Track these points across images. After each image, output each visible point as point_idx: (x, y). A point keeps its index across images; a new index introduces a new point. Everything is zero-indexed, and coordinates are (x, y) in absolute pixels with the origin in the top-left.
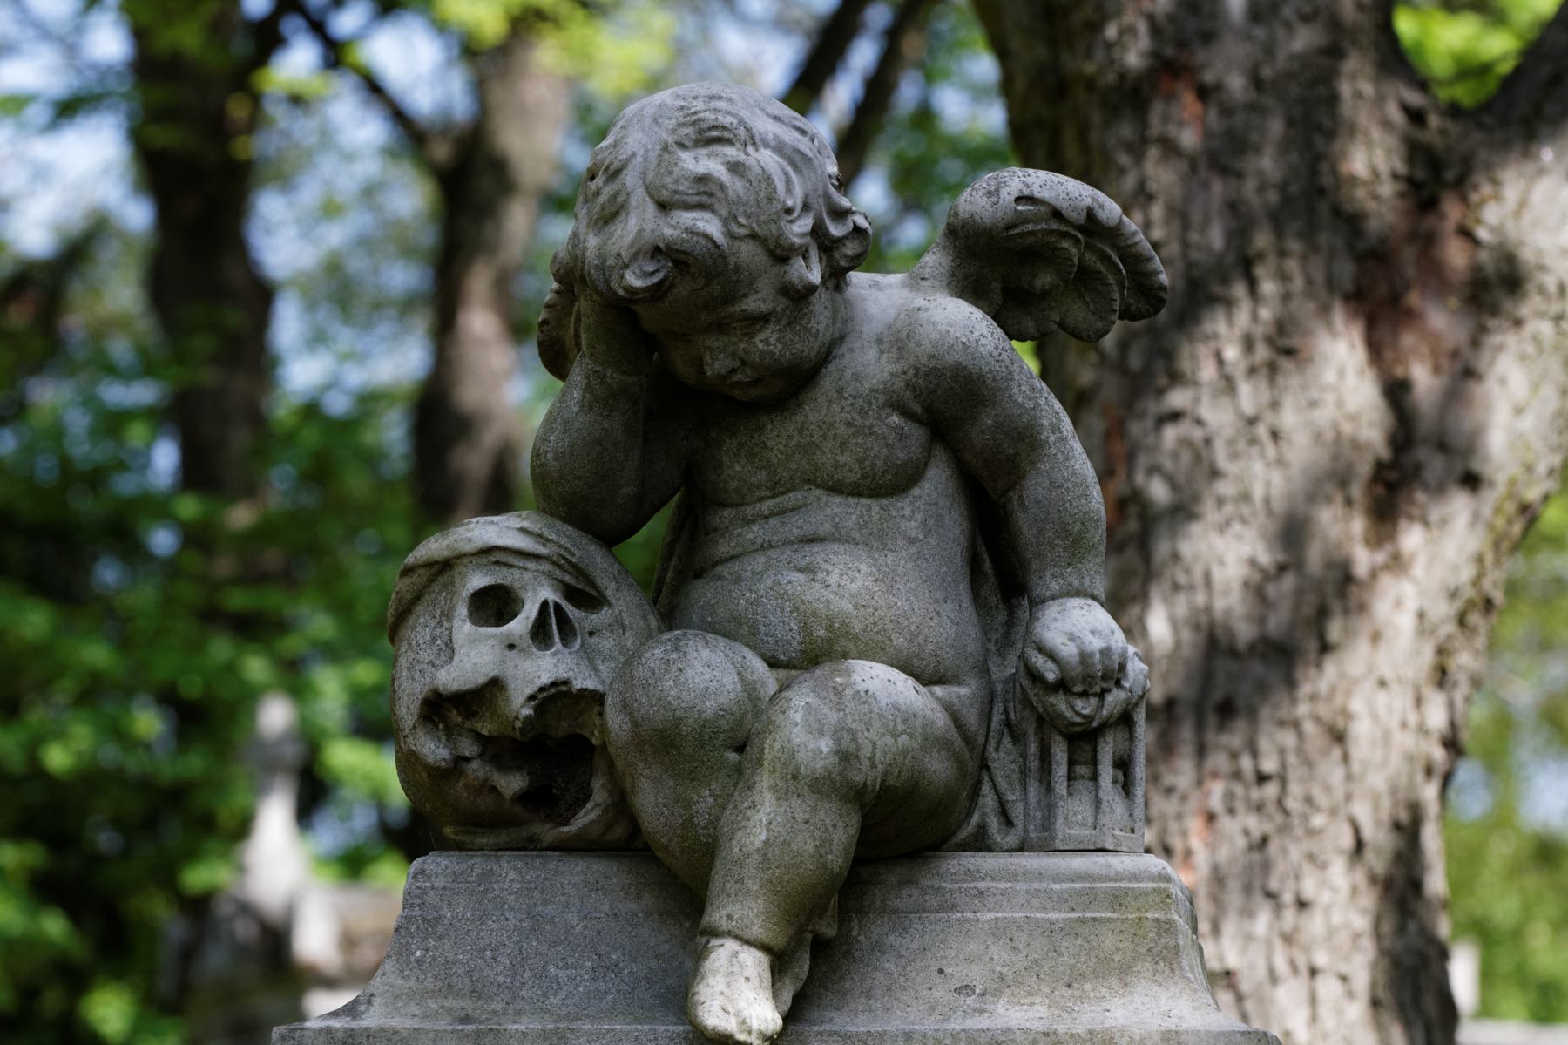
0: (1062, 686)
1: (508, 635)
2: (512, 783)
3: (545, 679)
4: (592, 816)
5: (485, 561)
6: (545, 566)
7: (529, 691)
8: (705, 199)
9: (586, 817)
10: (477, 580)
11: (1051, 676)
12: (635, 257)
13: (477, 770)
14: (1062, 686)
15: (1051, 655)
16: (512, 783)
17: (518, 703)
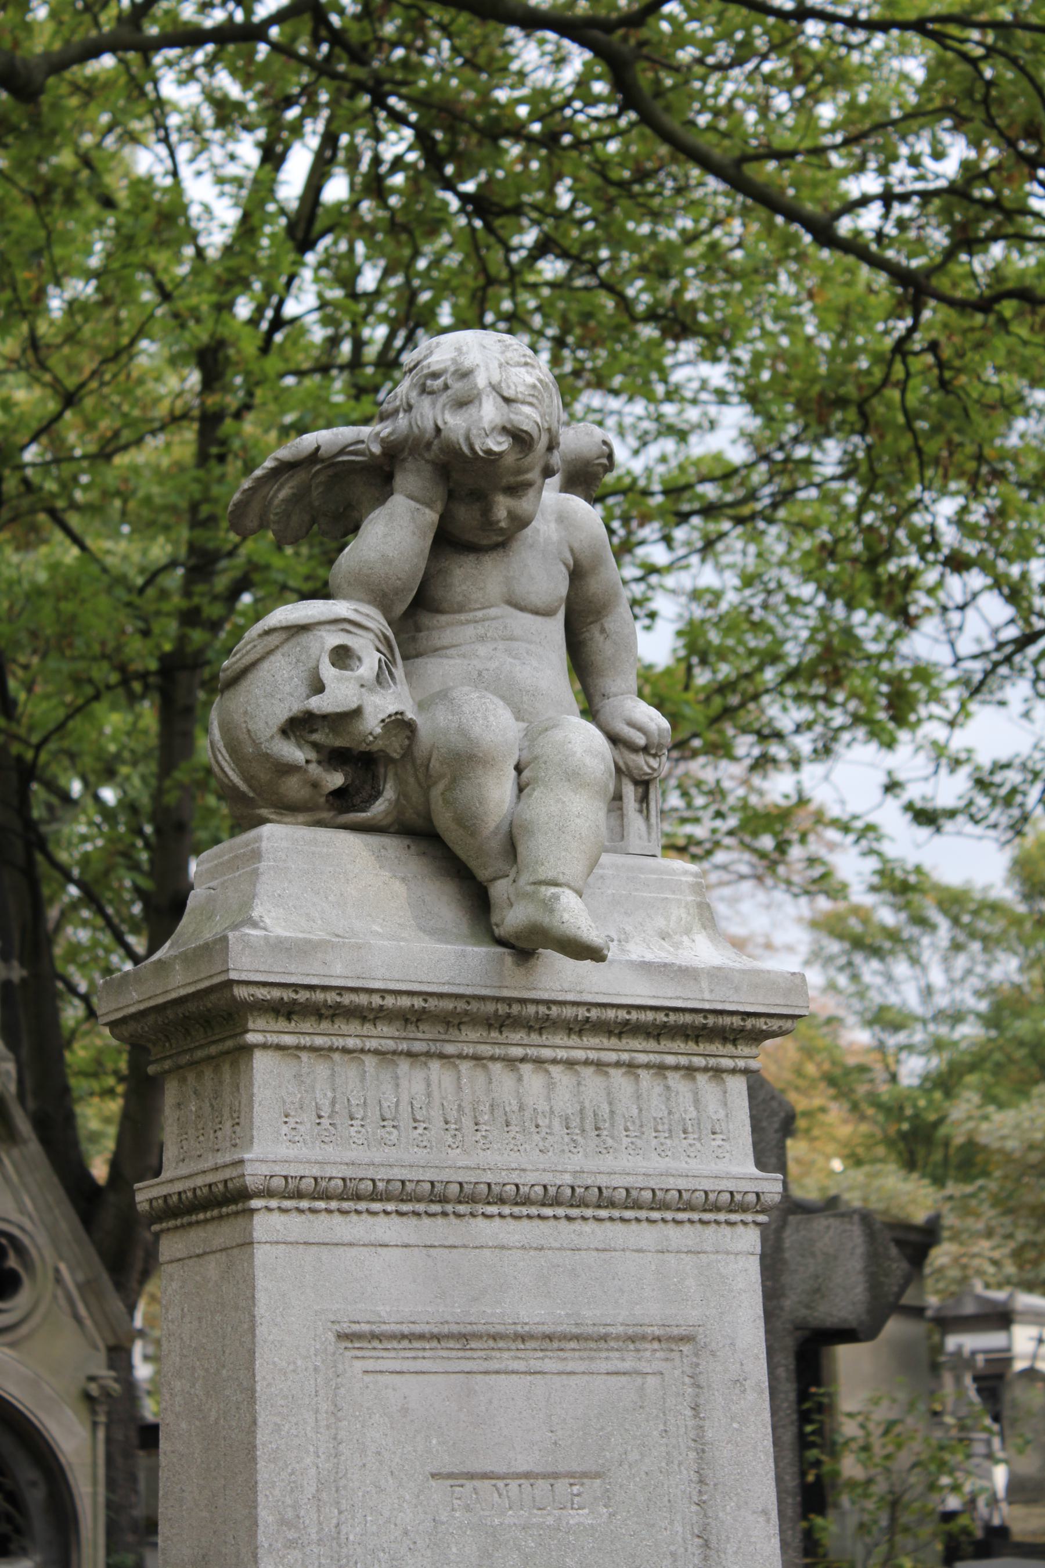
0: (645, 750)
1: (360, 678)
2: (336, 780)
3: (392, 709)
4: (382, 808)
5: (333, 627)
6: (371, 636)
7: (382, 716)
8: (534, 401)
9: (379, 808)
10: (333, 639)
11: (641, 740)
12: (493, 429)
13: (314, 769)
14: (645, 750)
15: (640, 729)
16: (336, 780)
17: (372, 723)
